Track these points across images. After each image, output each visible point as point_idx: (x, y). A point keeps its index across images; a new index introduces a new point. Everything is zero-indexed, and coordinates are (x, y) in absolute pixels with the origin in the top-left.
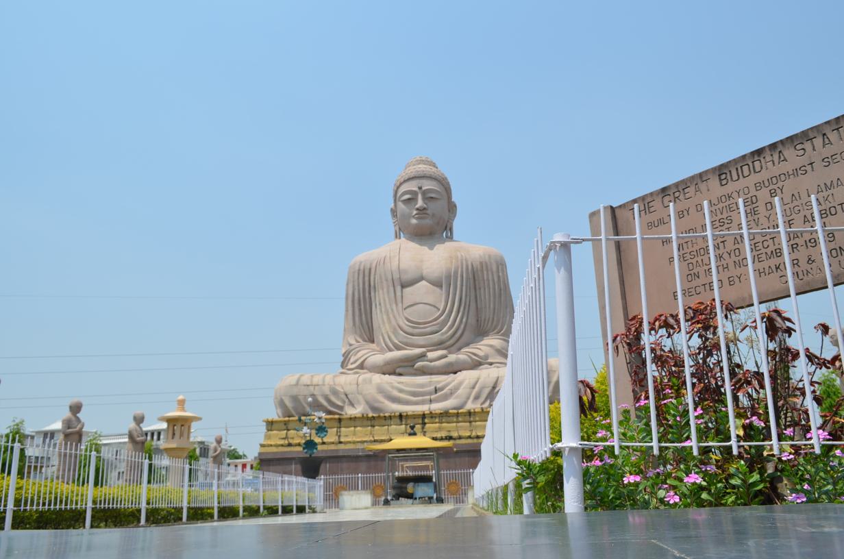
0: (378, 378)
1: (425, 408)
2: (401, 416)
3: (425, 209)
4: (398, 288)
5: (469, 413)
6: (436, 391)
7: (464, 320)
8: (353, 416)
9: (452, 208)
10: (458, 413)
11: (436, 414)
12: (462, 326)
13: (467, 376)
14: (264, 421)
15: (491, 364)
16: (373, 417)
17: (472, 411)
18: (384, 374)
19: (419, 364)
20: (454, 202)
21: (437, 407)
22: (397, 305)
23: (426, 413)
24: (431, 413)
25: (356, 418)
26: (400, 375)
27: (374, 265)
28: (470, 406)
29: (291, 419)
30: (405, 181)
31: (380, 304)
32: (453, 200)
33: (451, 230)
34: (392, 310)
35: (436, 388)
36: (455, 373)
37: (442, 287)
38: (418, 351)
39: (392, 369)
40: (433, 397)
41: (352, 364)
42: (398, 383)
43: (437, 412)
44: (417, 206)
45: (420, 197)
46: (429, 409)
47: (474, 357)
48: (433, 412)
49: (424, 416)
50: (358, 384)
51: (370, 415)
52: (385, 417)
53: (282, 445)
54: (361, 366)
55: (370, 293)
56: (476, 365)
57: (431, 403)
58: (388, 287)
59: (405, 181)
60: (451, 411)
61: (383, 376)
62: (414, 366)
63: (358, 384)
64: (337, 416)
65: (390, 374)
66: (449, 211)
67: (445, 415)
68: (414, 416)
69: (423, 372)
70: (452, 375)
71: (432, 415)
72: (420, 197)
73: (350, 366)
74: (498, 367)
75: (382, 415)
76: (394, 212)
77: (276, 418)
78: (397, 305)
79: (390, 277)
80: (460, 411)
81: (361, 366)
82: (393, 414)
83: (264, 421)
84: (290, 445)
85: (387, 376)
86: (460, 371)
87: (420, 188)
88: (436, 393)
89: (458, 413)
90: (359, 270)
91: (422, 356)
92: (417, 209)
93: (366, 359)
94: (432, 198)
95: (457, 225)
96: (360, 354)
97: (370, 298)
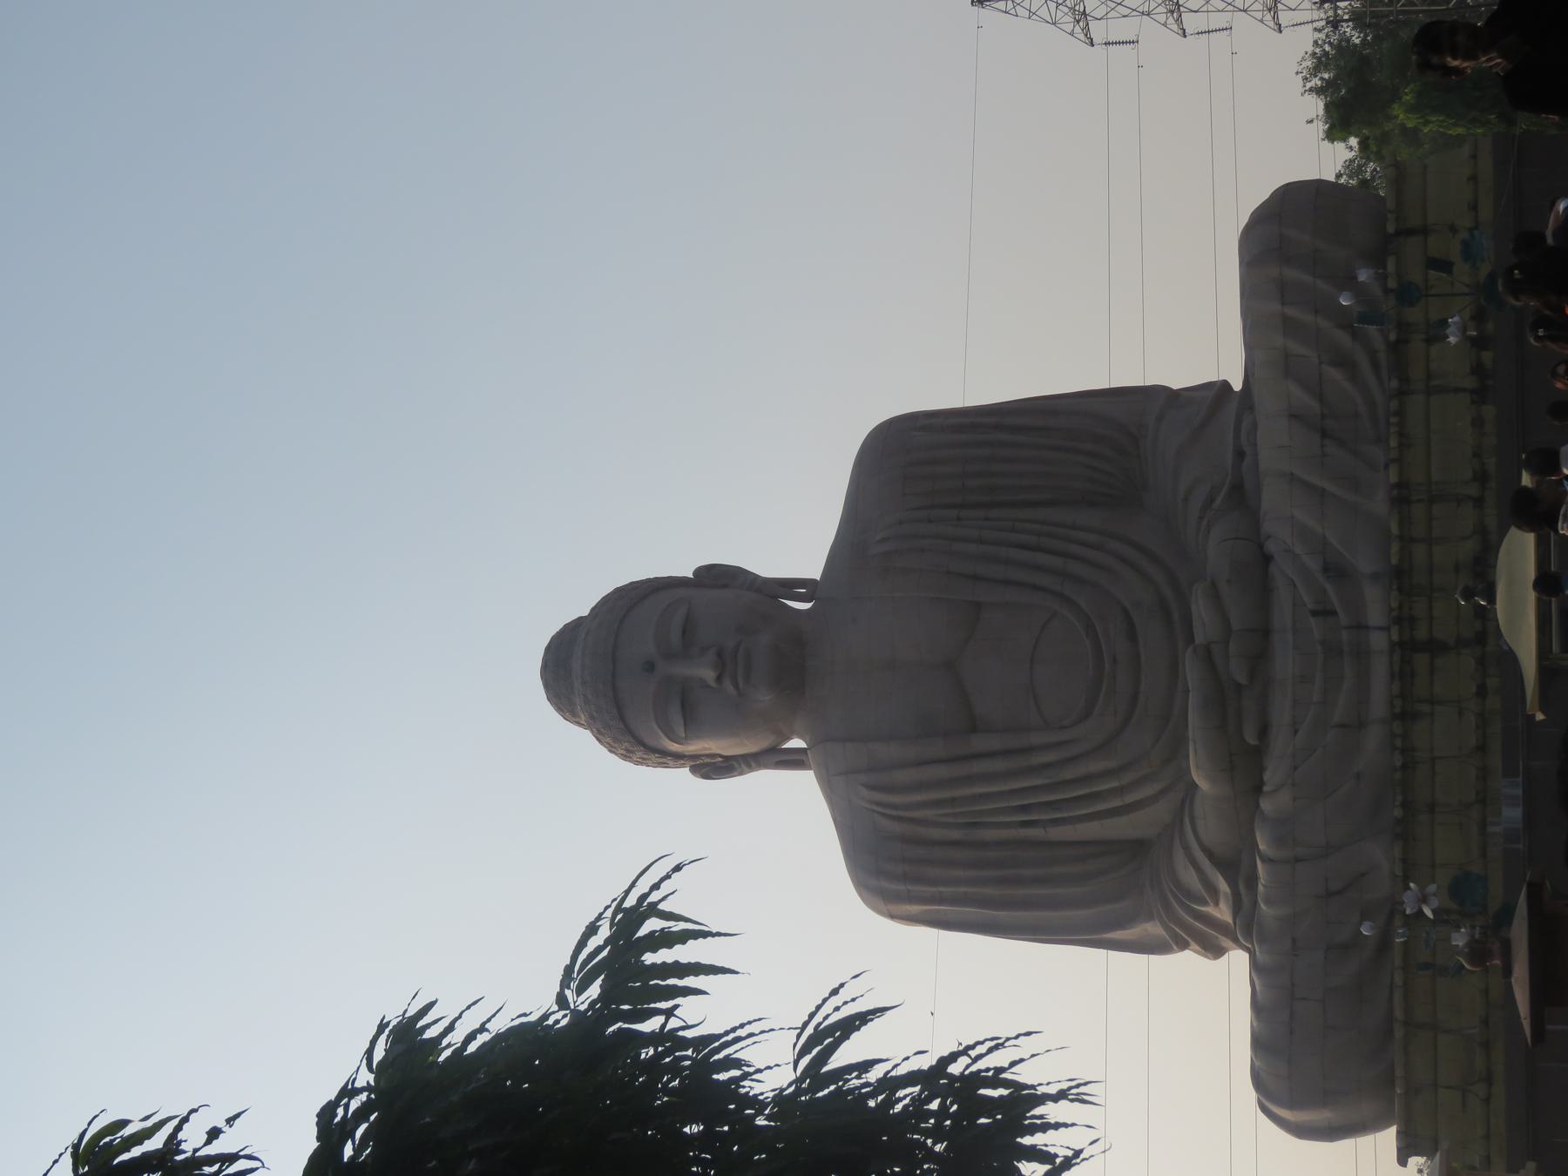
1: (1378, 641)
2: (1405, 714)
3: (720, 655)
4: (979, 743)
6: (1325, 612)
8: (1399, 872)
9: (715, 577)
10: (1401, 538)
11: (1400, 607)
13: (1283, 513)
14: (1403, 1162)
15: (1240, 454)
16: (1404, 805)
17: (1395, 492)
18: (1258, 789)
19: (1237, 671)
20: (698, 572)
21: (1376, 605)
22: (1031, 749)
23: (1395, 637)
24: (1398, 621)
25: (1404, 861)
26: (1264, 731)
27: (897, 828)
28: (1379, 504)
29: (1399, 1072)
30: (622, 718)
31: (1024, 809)
33: (788, 586)
35: (1315, 613)
36: (1267, 559)
38: (1192, 672)
40: (1343, 619)
41: (1217, 904)
42: (1296, 732)
43: (1394, 604)
44: (709, 675)
45: (682, 670)
46: (1381, 628)
48: (1395, 613)
49: (1406, 648)
50: (1297, 860)
51: (1398, 812)
52: (1404, 767)
53: (1487, 1100)
55: (984, 845)
56: (1240, 496)
57: (1367, 627)
58: (970, 779)
59: (622, 718)
60: (1394, 561)
61: (1266, 788)
62: (1239, 686)
63: (1297, 860)
65: (1262, 769)
66: (725, 586)
67: (1400, 577)
68: (1403, 675)
69: (1259, 658)
70: (1273, 569)
71: (1403, 619)
72: (682, 670)
73: (1223, 912)
74: (1255, 426)
75: (1398, 776)
77: (1392, 1132)
78: (1031, 749)
79: (942, 771)
80: (1395, 530)
82: (1398, 742)
83: (1403, 1162)
84: (1489, 1080)
85: (1267, 776)
86: (1261, 546)
87: (650, 667)
88: (1334, 613)
89: (1401, 538)
90: (905, 878)
91: (1207, 656)
92: (719, 679)
94: (684, 632)
95: (768, 565)
96: (1190, 878)
97: (1001, 844)
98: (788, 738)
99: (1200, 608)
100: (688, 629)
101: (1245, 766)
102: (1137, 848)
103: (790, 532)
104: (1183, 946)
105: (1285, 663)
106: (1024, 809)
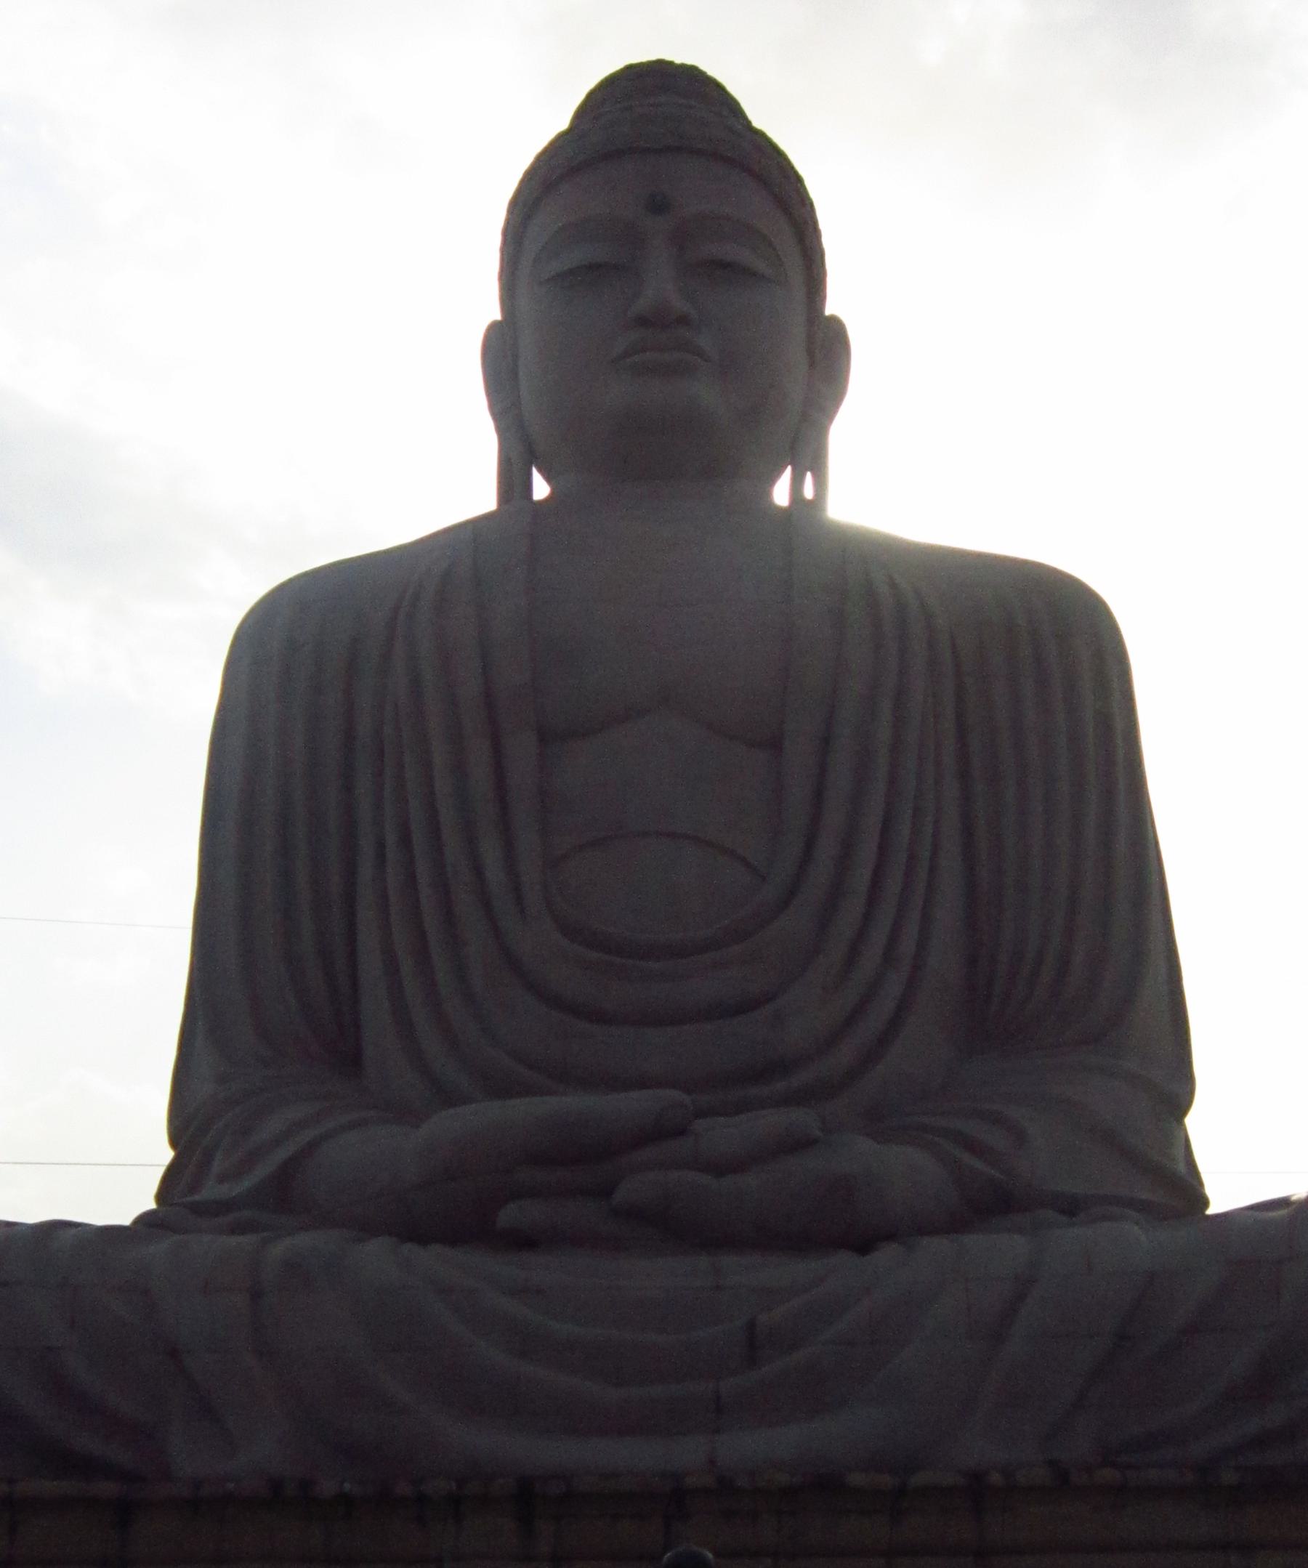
0: (377, 1258)
1: (687, 1454)
3: (683, 320)
5: (977, 1491)
7: (907, 945)
9: (827, 349)
12: (894, 986)
17: (996, 1478)
26: (523, 1241)
31: (405, 840)
32: (829, 310)
34: (478, 870)
36: (864, 1247)
37: (775, 744)
39: (456, 1212)
41: (222, 1179)
46: (712, 1462)
47: (968, 1159)
51: (327, 1488)
54: (283, 1196)
56: (992, 1203)
60: (856, 1479)
64: (107, 1488)
70: (844, 1259)
76: (501, 353)
81: (283, 1196)
85: (436, 1248)
86: (890, 1237)
92: (643, 321)
93: (311, 1148)
94: (725, 265)
98: (548, 479)
99: (769, 1122)
100: (729, 272)
101: (456, 1212)
102: (342, 1052)
103: (909, 462)
104: (174, 1141)
105: (656, 1275)
106: (405, 840)
